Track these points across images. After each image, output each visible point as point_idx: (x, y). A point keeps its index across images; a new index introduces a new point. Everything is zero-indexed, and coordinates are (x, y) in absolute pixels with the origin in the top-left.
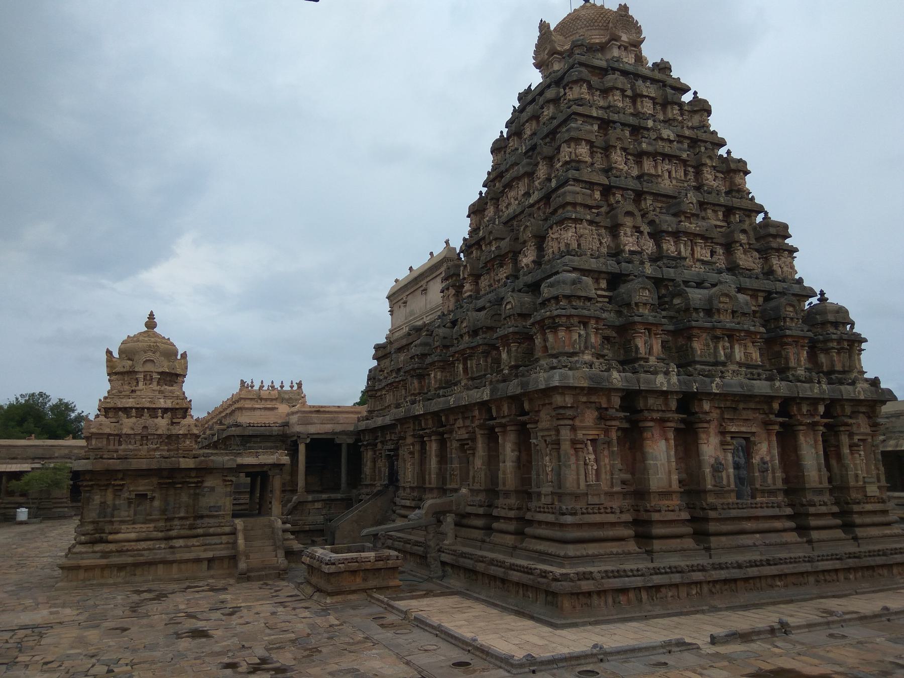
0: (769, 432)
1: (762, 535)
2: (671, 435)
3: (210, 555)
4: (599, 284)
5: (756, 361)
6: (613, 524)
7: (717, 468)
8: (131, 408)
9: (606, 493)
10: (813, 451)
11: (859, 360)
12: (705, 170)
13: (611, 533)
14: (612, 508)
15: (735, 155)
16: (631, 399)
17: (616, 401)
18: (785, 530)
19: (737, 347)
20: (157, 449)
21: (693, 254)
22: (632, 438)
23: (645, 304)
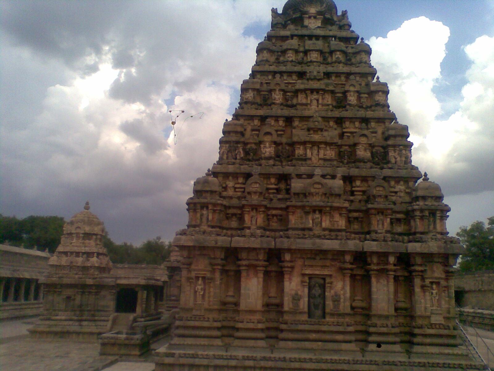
0: (344, 275)
1: (323, 343)
2: (261, 275)
3: (98, 331)
4: (237, 179)
5: (341, 226)
6: (209, 328)
7: (296, 298)
8: (68, 252)
9: (206, 310)
10: (385, 288)
11: (444, 225)
12: (348, 94)
13: (203, 333)
14: (209, 318)
15: (382, 80)
16: (232, 253)
17: (220, 255)
18: (394, 343)
19: (324, 218)
20: (76, 274)
21: (318, 155)
22: (234, 277)
23: (255, 193)
